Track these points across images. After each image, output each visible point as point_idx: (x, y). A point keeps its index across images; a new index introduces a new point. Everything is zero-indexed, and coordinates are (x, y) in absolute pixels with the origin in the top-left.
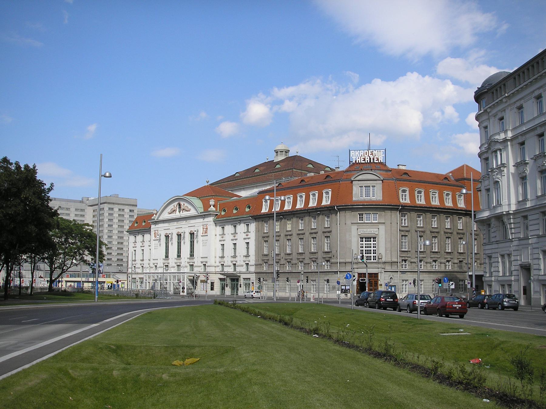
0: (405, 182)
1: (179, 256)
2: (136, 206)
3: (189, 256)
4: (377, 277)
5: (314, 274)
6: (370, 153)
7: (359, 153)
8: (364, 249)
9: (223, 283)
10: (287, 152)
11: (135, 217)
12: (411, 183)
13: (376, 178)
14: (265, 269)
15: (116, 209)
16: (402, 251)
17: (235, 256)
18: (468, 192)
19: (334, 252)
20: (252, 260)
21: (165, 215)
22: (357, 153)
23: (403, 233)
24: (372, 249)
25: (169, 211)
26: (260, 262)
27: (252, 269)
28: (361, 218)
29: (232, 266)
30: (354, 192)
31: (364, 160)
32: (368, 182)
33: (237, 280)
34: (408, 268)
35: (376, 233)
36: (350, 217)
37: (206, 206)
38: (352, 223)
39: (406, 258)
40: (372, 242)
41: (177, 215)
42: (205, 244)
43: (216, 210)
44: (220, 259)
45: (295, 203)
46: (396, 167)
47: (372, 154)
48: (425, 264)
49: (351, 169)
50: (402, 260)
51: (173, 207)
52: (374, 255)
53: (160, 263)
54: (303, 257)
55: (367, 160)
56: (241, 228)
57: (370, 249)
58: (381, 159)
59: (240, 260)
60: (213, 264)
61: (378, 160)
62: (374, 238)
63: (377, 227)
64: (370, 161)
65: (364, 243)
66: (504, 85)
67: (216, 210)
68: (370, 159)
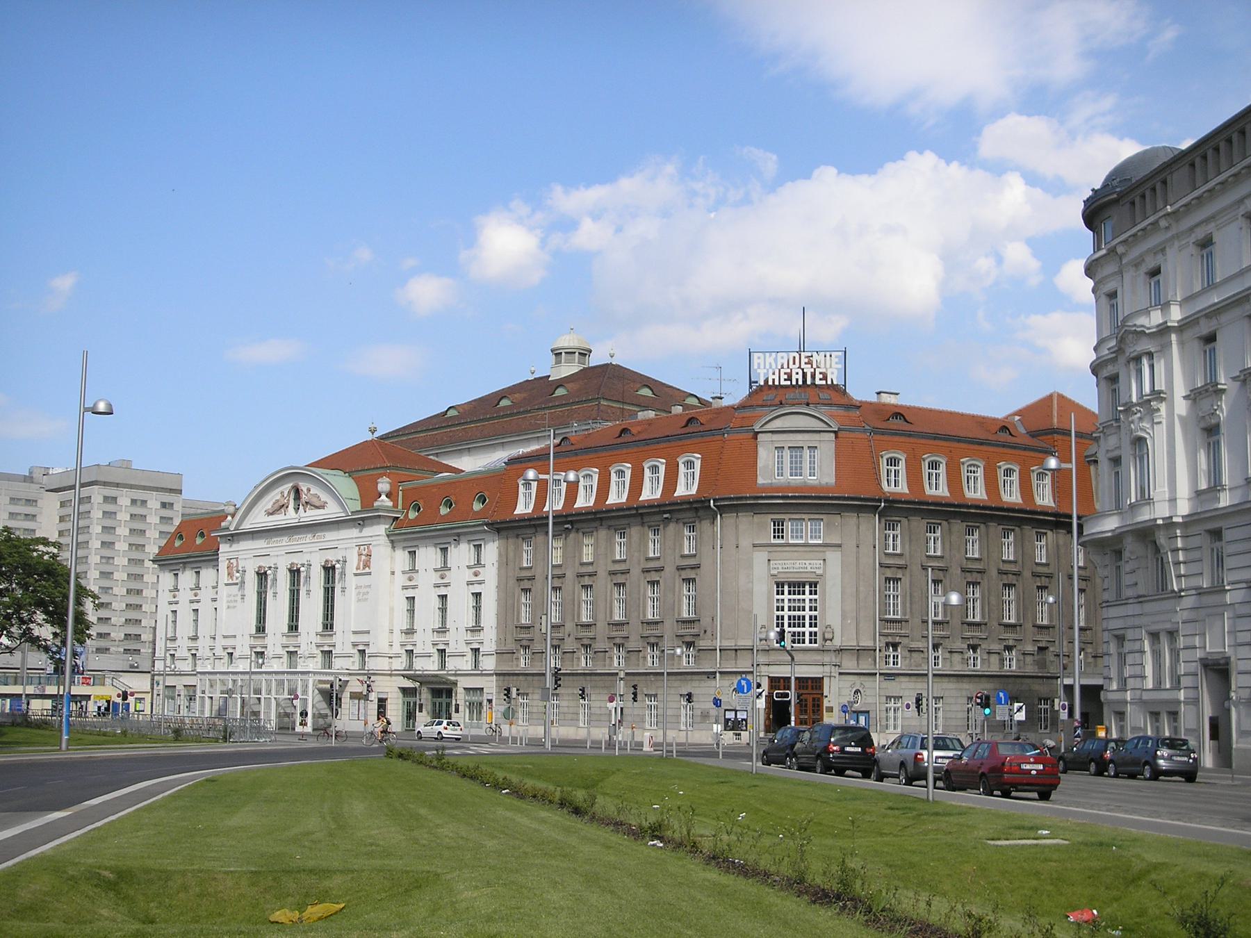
0: (897, 438)
1: (293, 628)
2: (180, 492)
3: (320, 629)
4: (821, 688)
5: (652, 678)
6: (804, 360)
7: (776, 360)
8: (786, 613)
9: (412, 700)
10: (585, 353)
11: (177, 522)
12: (912, 440)
13: (819, 425)
14: (522, 664)
15: (124, 499)
16: (887, 621)
17: (443, 630)
18: (1064, 466)
19: (706, 621)
20: (489, 639)
21: (258, 519)
22: (770, 359)
23: (889, 573)
24: (807, 613)
25: (269, 506)
26: (511, 646)
27: (489, 664)
28: (779, 533)
29: (436, 656)
30: (761, 463)
31: (789, 378)
32: (799, 437)
33: (449, 693)
34: (901, 666)
35: (819, 572)
36: (749, 530)
37: (368, 495)
38: (754, 546)
39: (897, 639)
40: (807, 597)
41: (290, 517)
42: (362, 597)
43: (395, 506)
44: (403, 638)
46: (873, 398)
47: (809, 363)
48: (948, 655)
49: (754, 403)
50: (887, 644)
51: (278, 497)
52: (813, 629)
53: (243, 646)
55: (797, 377)
56: (461, 554)
57: (801, 613)
58: (834, 377)
59: (457, 640)
60: (385, 649)
61: (825, 378)
63: (821, 555)
65: (786, 597)
66: (1164, 182)
67: (395, 506)
68: (804, 375)
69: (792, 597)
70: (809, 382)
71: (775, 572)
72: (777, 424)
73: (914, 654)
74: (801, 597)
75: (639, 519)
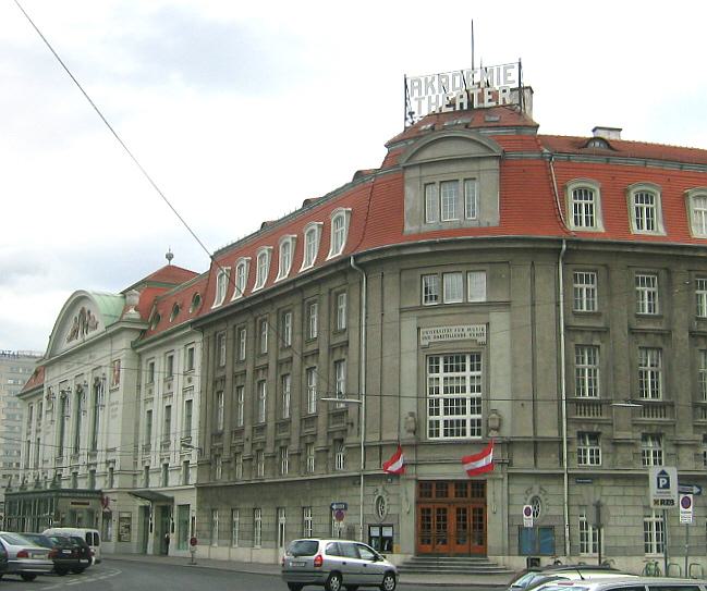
4: (483, 495)
13: (474, 150)
14: (221, 477)
16: (579, 403)
23: (580, 340)
30: (407, 208)
32: (453, 168)
34: (605, 465)
35: (482, 339)
36: (388, 293)
39: (595, 428)
40: (468, 373)
48: (672, 450)
50: (581, 435)
57: (460, 395)
62: (476, 357)
63: (483, 318)
64: (470, 104)
65: (441, 375)
69: (449, 374)
70: (476, 105)
71: (424, 343)
73: (622, 450)
74: (461, 374)
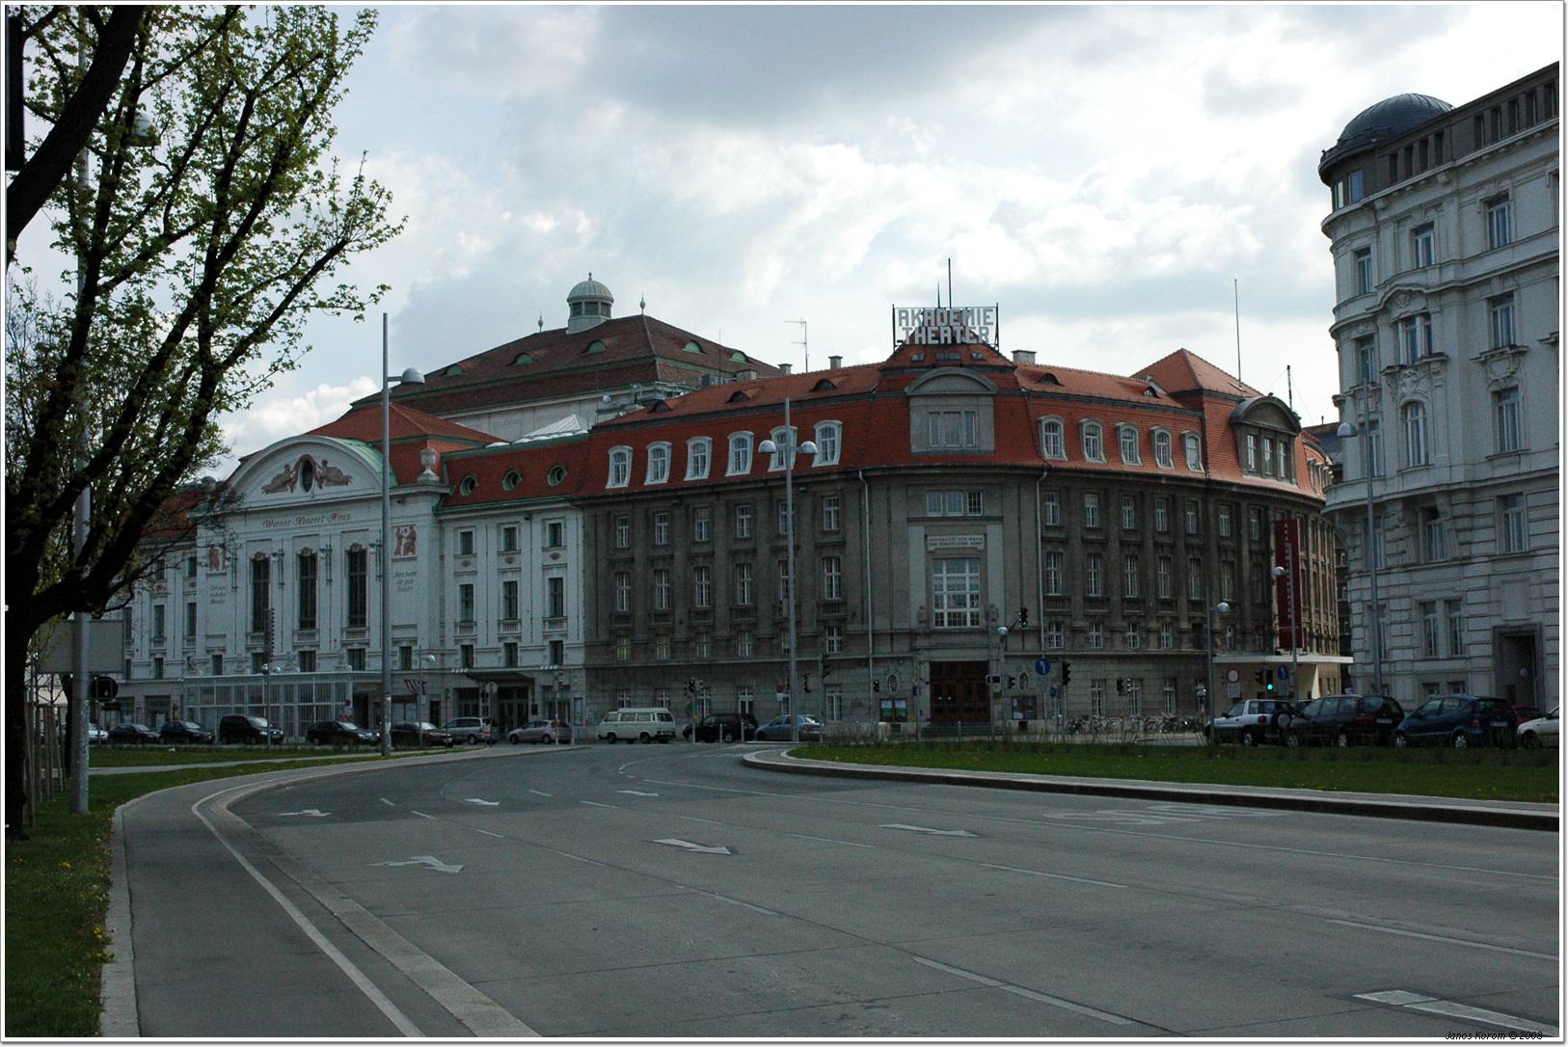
3: (250, 629)
16: (1051, 599)
19: (854, 601)
20: (575, 628)
23: (1049, 548)
25: (268, 482)
26: (604, 637)
27: (575, 658)
30: (913, 432)
31: (937, 338)
33: (523, 693)
35: (981, 547)
45: (678, 466)
53: (238, 647)
54: (751, 619)
56: (532, 537)
64: (954, 339)
66: (1439, 136)
72: (931, 388)
75: (765, 494)
